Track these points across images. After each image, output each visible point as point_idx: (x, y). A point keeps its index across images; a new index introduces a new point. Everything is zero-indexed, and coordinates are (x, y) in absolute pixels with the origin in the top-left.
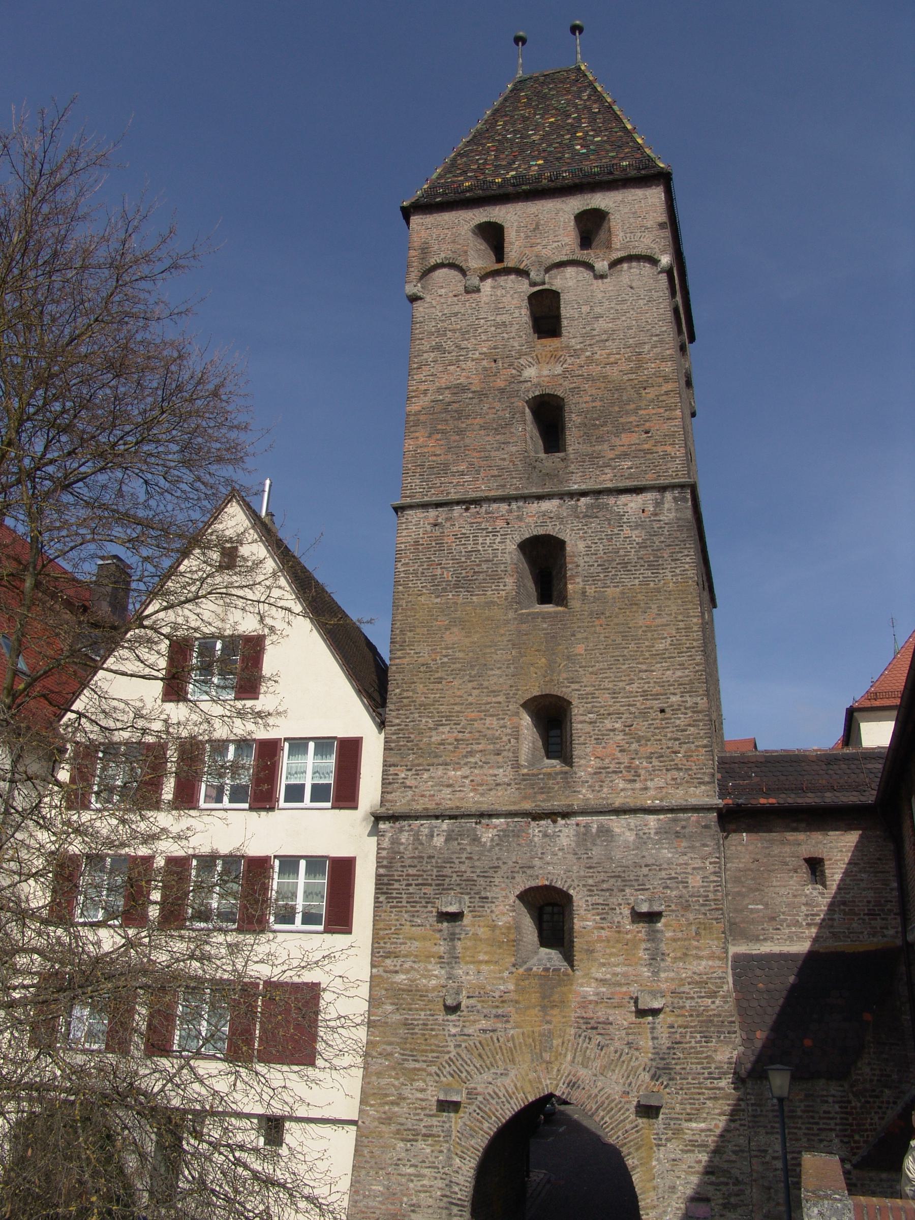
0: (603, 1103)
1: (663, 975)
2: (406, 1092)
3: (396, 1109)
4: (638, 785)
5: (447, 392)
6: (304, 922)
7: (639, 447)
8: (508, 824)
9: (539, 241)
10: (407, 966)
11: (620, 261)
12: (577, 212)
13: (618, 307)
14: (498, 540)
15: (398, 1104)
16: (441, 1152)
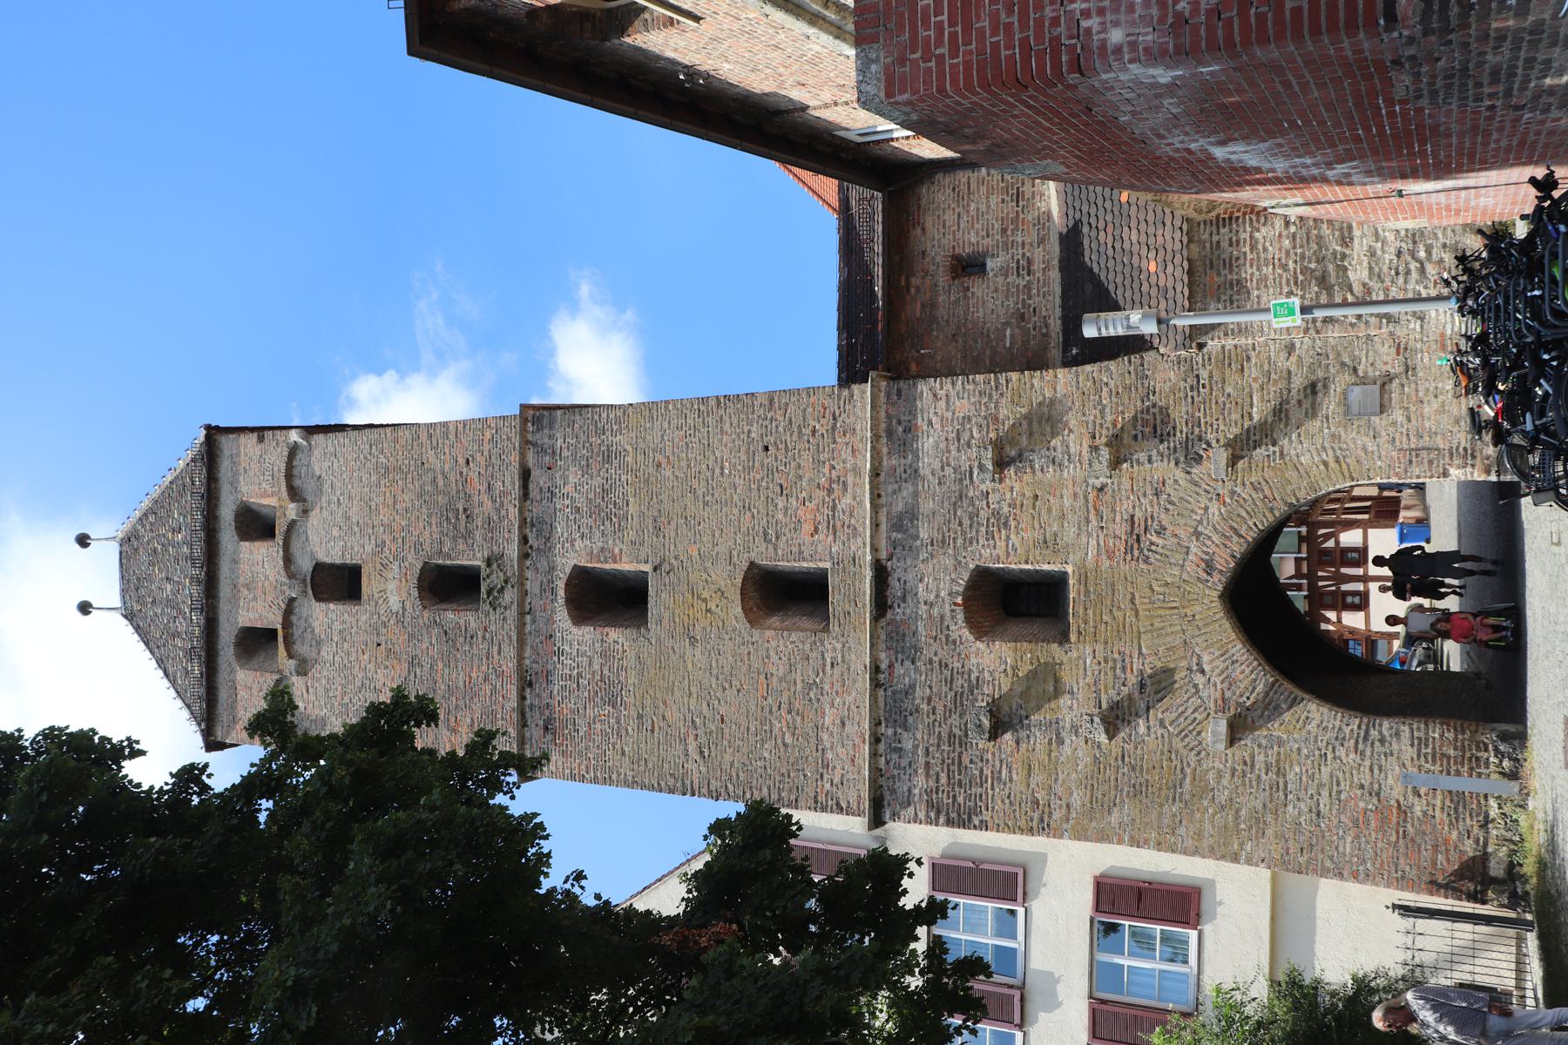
0: (1231, 528)
1: (1072, 450)
2: (1223, 797)
3: (1243, 812)
4: (850, 479)
6: (1013, 936)
10: (1059, 790)
15: (1238, 811)
16: (1299, 749)
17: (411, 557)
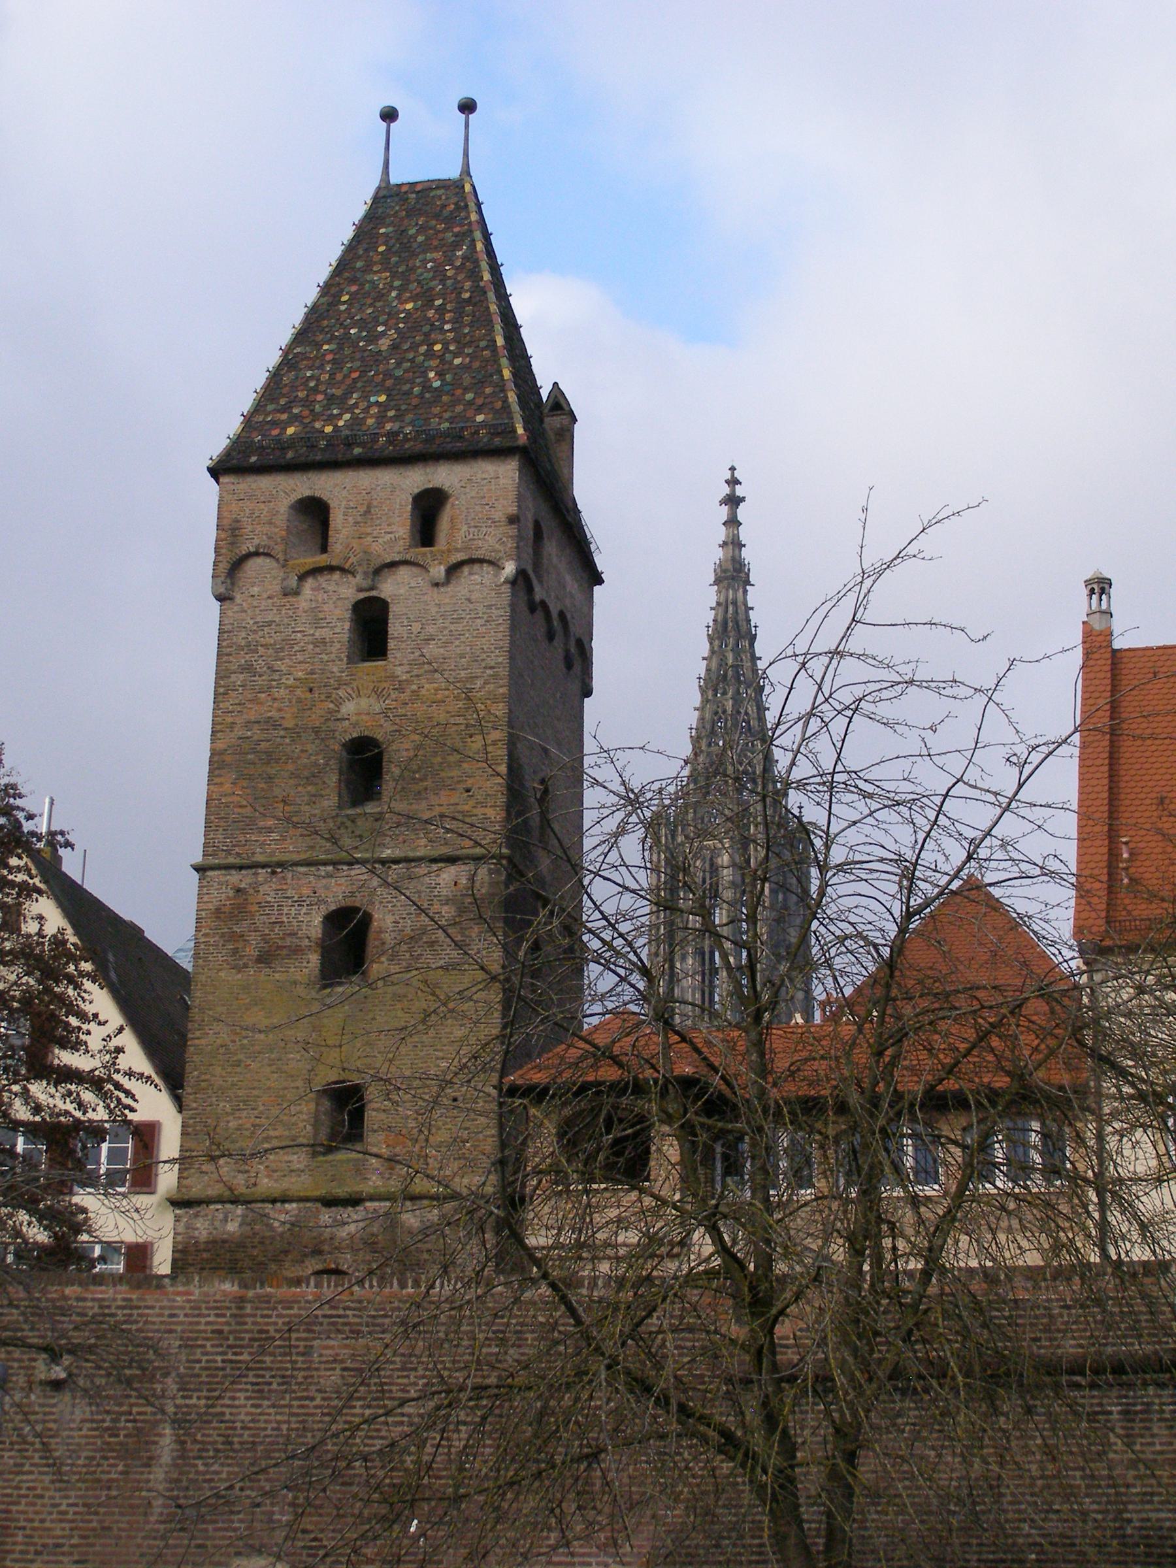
5: (256, 726)
7: (459, 808)
8: (299, 1210)
9: (369, 530)
11: (461, 564)
12: (416, 491)
13: (452, 627)
14: (304, 910)
17: (388, 727)
